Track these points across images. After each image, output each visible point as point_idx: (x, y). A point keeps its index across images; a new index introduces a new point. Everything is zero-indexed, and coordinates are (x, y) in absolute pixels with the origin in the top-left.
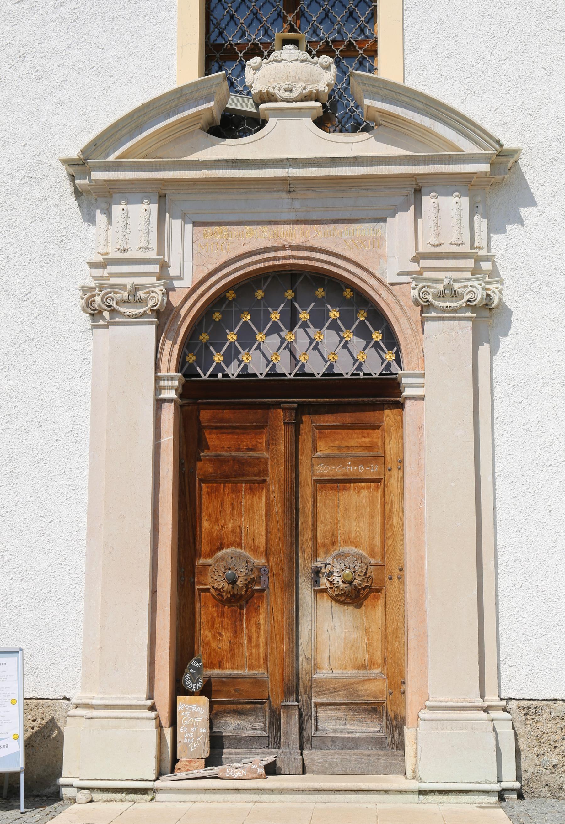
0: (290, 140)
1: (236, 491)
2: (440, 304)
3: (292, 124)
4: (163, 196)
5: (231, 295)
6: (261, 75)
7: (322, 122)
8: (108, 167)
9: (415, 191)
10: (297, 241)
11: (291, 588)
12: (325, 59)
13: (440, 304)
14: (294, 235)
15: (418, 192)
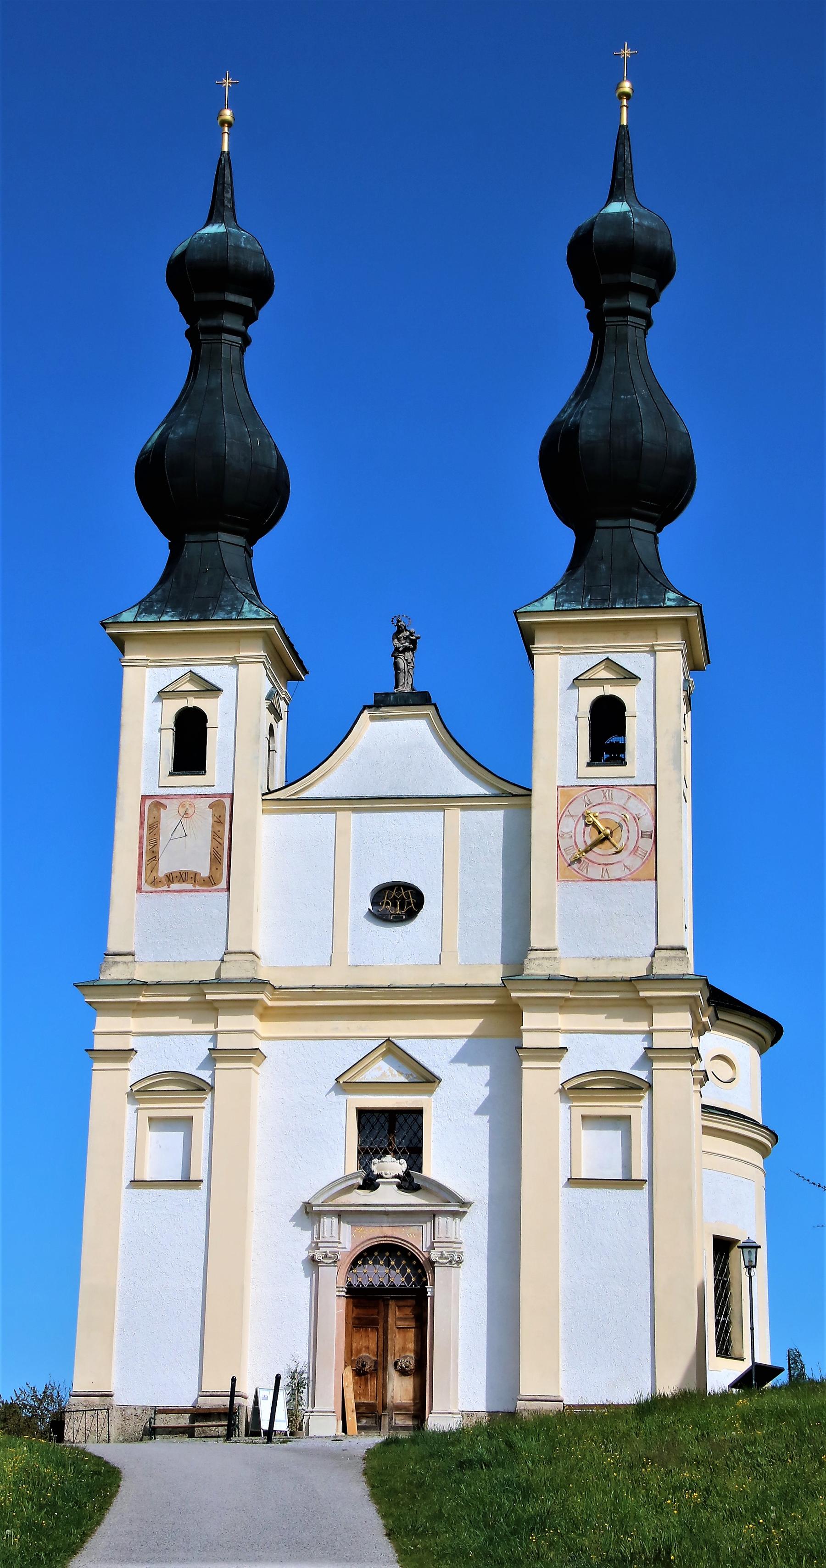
0: (388, 1195)
1: (366, 1331)
2: (441, 1261)
3: (389, 1187)
4: (340, 1215)
5: (365, 1254)
6: (377, 1166)
7: (400, 1187)
8: (319, 1205)
9: (434, 1215)
10: (389, 1234)
11: (385, 1368)
12: (402, 1161)
13: (441, 1261)
14: (388, 1231)
15: (434, 1216)
